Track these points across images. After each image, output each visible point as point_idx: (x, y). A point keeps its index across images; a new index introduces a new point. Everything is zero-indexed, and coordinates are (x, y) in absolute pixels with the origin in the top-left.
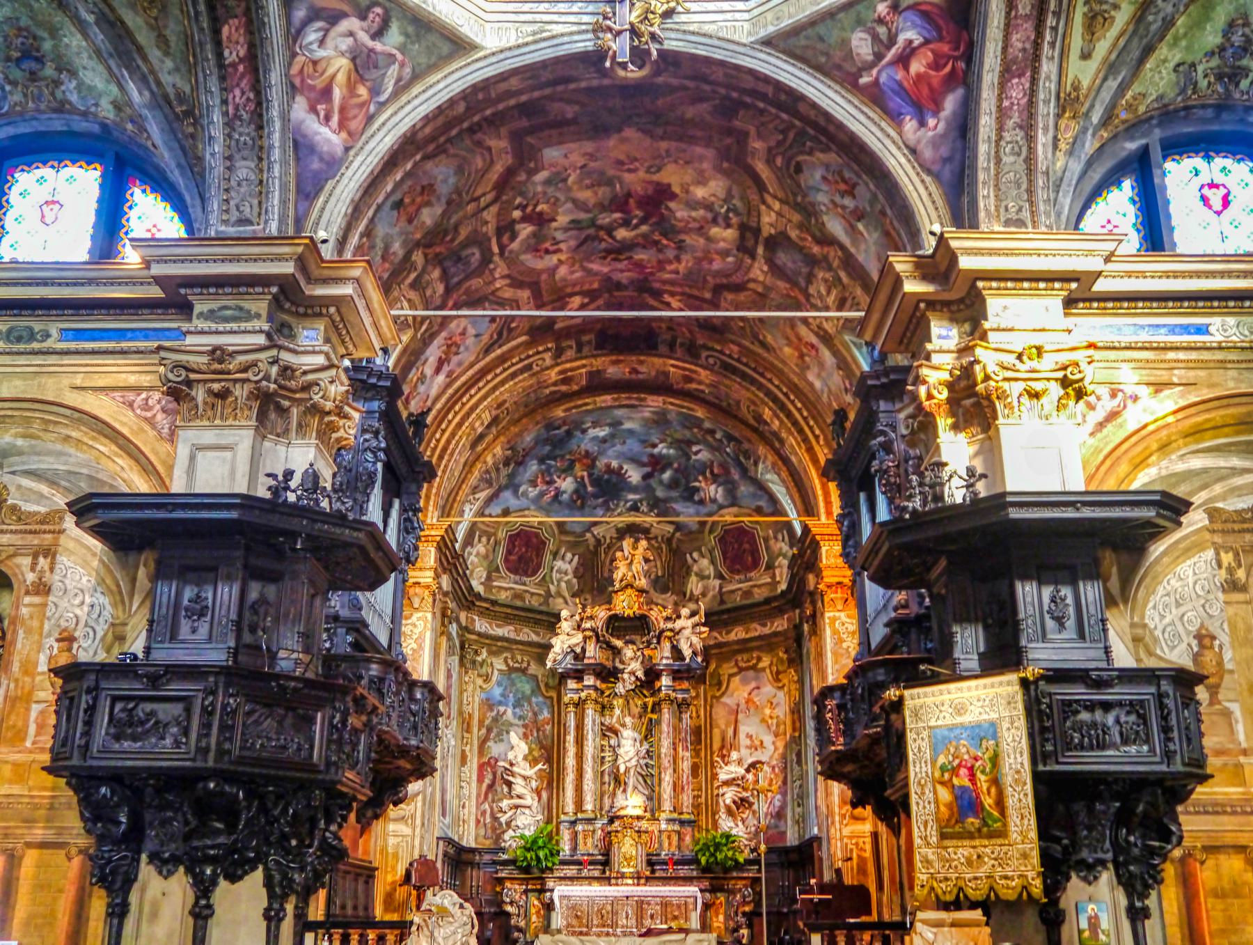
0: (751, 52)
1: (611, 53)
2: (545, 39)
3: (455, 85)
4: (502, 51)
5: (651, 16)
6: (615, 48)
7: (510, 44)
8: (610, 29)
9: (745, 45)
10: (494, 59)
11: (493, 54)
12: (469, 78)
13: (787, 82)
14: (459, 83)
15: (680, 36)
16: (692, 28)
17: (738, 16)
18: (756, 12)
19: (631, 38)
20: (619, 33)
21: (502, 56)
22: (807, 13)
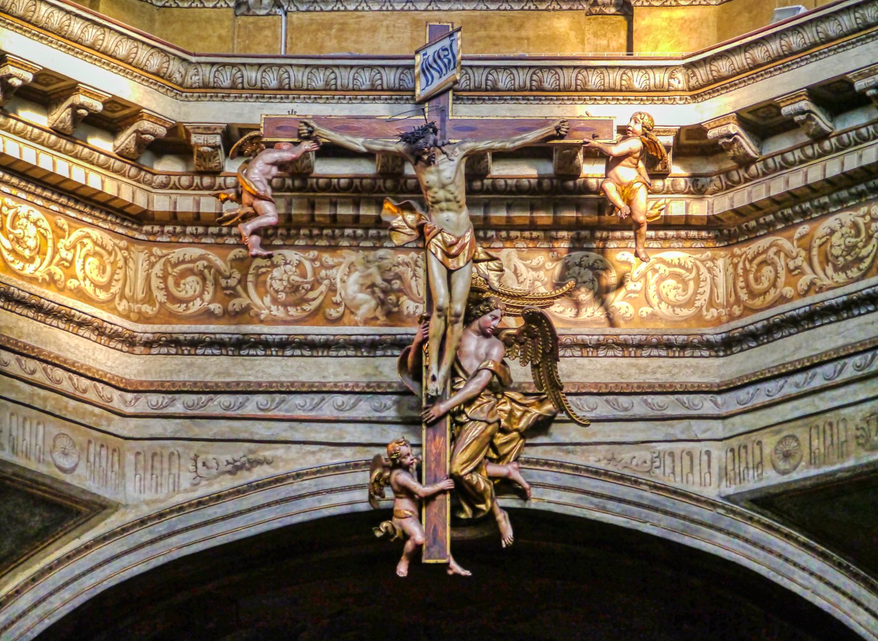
0: (726, 521)
1: (409, 545)
2: (259, 486)
3: (56, 600)
4: (161, 515)
5: (500, 439)
6: (418, 534)
7: (179, 499)
8: (405, 492)
9: (713, 505)
10: (142, 535)
11: (142, 522)
12: (88, 581)
13: (808, 596)
14: (66, 594)
15: (567, 480)
16: (592, 459)
17: (698, 428)
18: (741, 423)
19: (456, 508)
20: (429, 499)
21: (161, 528)
22: (850, 463)
